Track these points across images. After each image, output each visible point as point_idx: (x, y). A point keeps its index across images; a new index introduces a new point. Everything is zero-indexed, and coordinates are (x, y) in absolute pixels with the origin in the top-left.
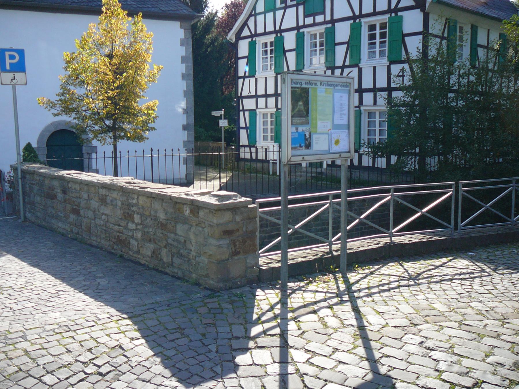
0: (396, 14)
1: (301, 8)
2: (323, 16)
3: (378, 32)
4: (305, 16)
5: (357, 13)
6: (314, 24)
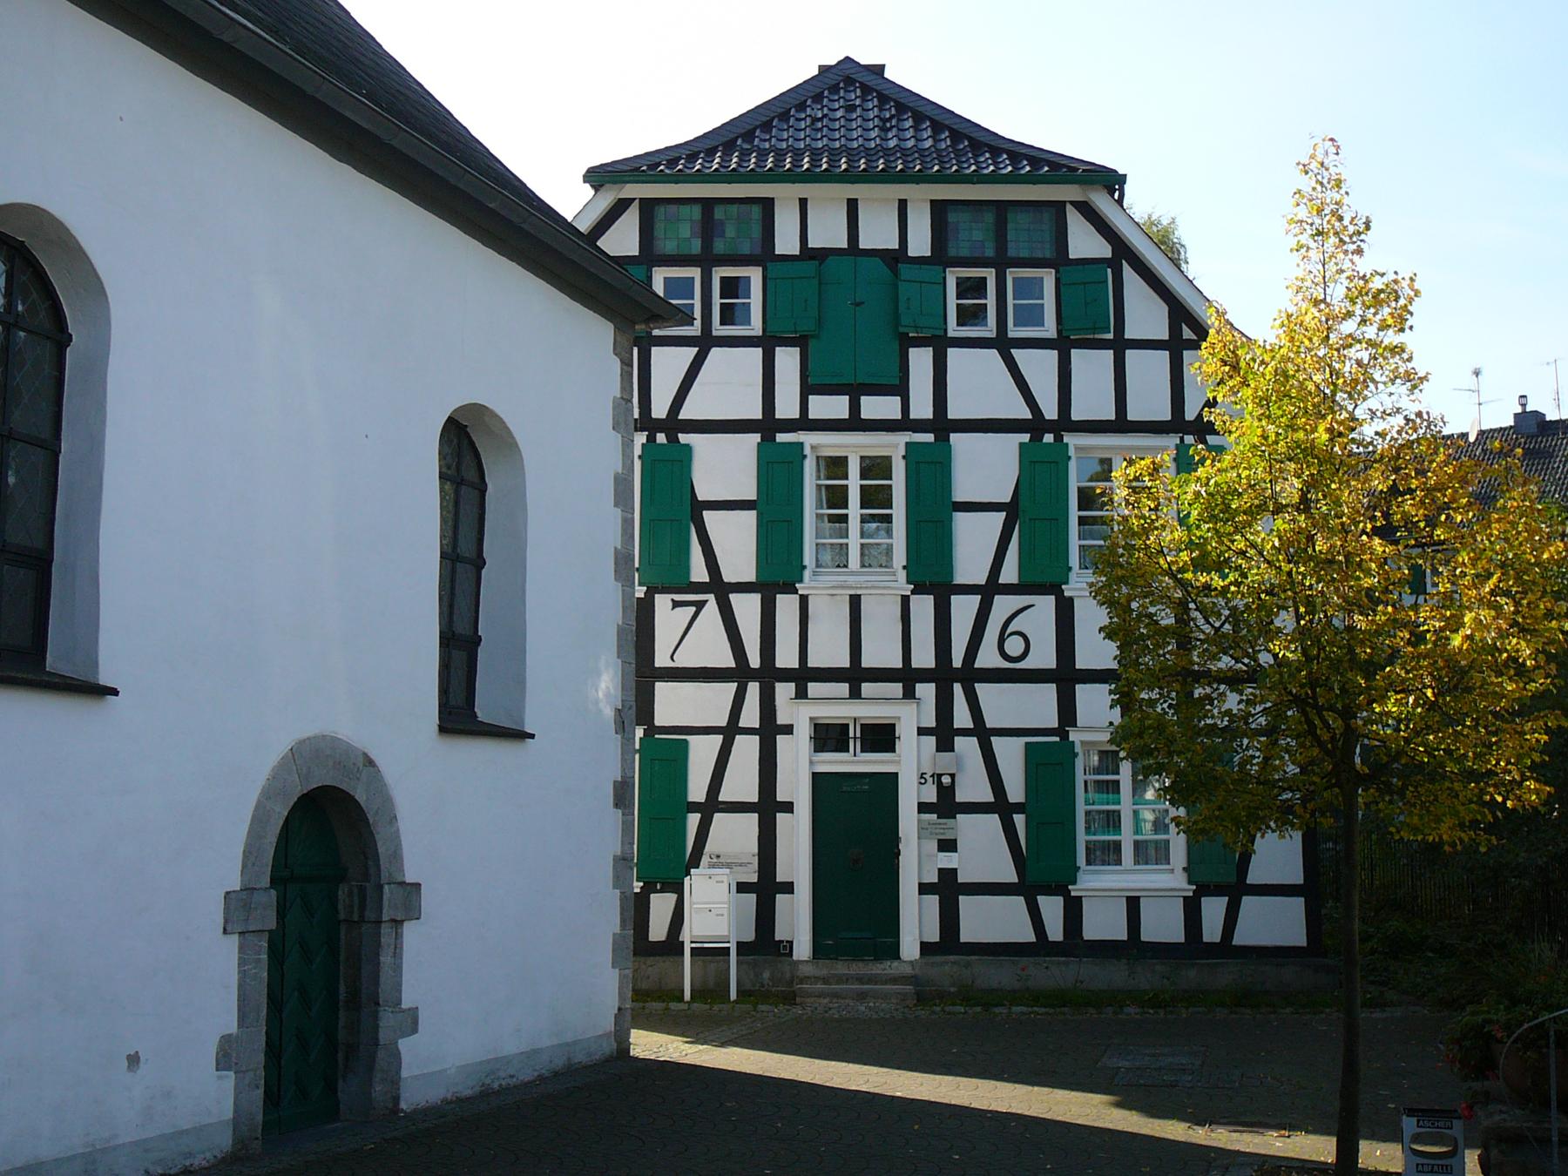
0: (673, 439)
1: (788, 361)
2: (896, 401)
3: (854, 483)
4: (807, 389)
5: (1051, 412)
6: (854, 423)
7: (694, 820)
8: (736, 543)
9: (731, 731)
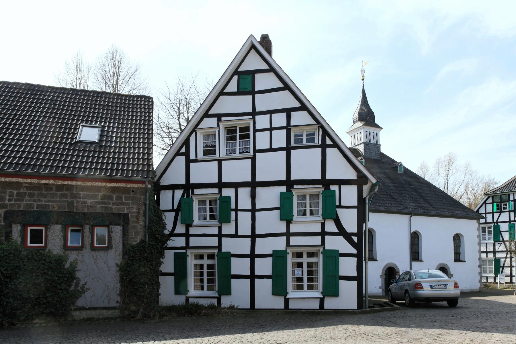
7: (501, 268)
8: (506, 236)
9: (506, 258)
